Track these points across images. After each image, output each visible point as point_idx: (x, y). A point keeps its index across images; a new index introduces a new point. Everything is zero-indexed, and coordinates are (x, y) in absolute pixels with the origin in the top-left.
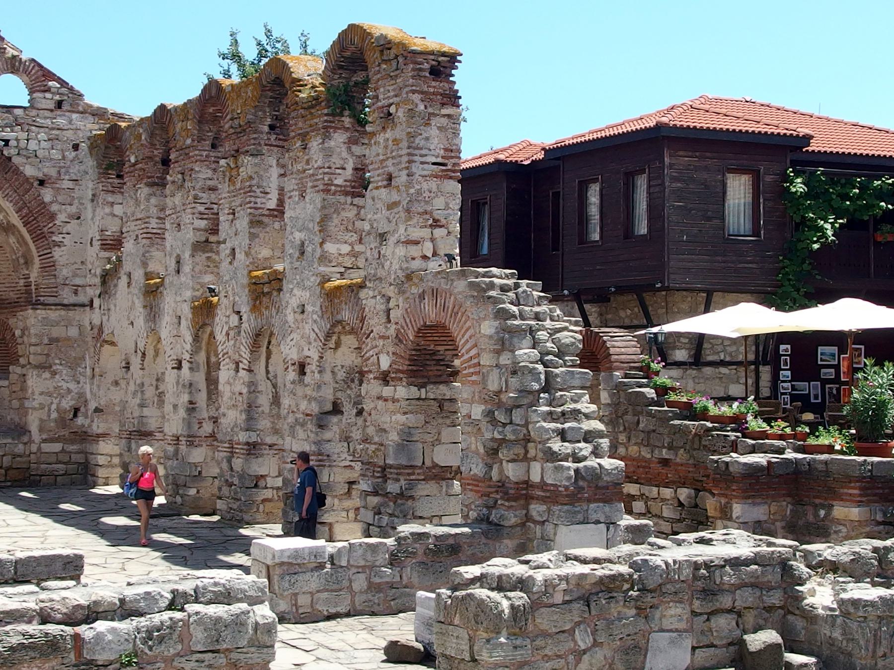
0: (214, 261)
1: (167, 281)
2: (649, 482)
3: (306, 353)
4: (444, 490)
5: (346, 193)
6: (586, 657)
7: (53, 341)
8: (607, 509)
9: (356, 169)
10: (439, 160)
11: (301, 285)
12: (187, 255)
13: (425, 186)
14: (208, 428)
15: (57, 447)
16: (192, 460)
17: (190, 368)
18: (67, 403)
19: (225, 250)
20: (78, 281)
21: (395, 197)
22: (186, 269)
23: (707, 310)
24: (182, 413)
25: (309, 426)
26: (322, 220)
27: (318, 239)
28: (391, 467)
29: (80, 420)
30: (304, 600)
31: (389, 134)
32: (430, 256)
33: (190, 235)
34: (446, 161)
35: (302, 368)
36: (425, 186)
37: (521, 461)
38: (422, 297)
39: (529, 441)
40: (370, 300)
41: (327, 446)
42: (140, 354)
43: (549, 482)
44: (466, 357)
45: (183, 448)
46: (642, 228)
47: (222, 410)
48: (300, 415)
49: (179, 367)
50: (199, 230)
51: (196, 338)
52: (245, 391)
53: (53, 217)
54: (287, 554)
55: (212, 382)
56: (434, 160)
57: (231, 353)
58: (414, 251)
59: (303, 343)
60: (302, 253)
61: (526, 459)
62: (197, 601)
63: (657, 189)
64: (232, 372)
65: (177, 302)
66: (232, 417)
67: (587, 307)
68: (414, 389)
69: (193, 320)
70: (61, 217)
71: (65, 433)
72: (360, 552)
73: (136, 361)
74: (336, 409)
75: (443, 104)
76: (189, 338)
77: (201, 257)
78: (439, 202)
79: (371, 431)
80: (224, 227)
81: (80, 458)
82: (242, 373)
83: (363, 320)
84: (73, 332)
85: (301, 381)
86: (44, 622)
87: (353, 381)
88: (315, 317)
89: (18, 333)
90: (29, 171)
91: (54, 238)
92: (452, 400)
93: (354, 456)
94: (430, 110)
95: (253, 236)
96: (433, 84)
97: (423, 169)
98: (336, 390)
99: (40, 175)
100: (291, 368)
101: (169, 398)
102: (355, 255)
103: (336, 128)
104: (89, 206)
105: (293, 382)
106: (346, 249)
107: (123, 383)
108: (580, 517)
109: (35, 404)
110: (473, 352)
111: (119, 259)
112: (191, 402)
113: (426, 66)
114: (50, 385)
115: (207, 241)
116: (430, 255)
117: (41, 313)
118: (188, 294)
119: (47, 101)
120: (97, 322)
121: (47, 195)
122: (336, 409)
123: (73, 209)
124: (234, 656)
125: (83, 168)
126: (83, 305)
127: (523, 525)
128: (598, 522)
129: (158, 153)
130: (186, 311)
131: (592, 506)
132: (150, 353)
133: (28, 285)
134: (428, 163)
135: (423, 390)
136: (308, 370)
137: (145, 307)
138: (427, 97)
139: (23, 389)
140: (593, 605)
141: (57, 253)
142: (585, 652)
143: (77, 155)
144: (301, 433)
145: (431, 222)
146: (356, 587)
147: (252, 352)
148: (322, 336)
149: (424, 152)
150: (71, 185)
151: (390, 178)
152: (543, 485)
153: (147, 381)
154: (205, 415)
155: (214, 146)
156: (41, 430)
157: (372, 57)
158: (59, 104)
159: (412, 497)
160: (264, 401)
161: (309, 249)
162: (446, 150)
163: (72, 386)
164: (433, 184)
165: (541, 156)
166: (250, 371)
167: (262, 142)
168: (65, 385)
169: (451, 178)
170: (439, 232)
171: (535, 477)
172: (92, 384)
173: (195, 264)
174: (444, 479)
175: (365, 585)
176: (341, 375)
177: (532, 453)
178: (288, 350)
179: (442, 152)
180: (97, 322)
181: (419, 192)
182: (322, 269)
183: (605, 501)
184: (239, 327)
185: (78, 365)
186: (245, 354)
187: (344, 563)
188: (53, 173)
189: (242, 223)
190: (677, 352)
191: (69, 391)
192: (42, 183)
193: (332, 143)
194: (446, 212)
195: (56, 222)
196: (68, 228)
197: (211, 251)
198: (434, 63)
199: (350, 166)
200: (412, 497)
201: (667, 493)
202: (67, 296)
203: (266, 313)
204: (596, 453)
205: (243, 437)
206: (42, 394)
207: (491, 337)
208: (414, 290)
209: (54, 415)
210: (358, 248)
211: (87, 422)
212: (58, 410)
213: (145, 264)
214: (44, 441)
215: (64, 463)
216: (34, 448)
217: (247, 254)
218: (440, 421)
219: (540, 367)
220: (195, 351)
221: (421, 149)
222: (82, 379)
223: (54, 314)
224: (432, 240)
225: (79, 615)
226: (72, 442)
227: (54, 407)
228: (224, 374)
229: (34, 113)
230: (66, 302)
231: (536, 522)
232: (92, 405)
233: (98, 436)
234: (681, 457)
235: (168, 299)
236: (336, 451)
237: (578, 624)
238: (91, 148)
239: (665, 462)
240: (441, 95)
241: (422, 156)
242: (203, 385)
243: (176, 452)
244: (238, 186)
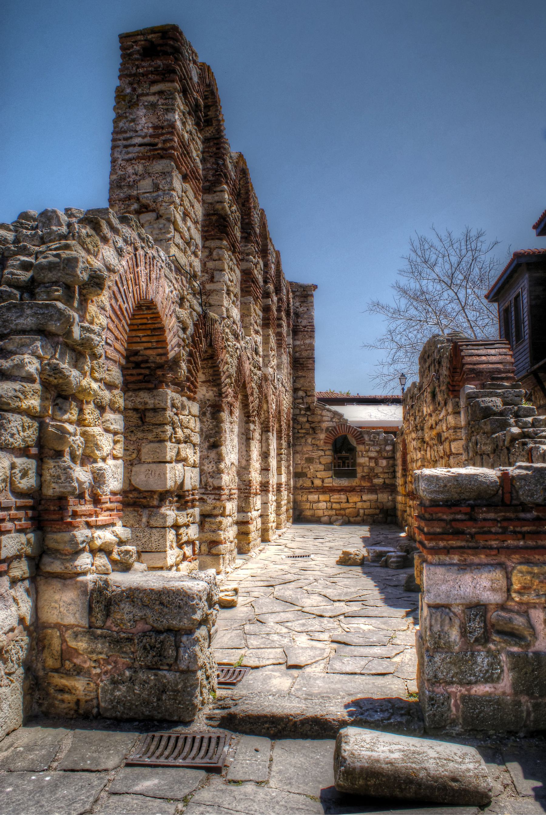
4: (144, 520)
34: (156, 140)
36: (130, 170)
75: (153, 83)
92: (155, 410)
93: (206, 489)
94: (140, 91)
96: (144, 64)
97: (128, 153)
134: (134, 145)
145: (135, 206)
149: (128, 135)
162: (155, 128)
174: (145, 507)
179: (151, 131)
194: (155, 194)
198: (143, 43)
218: (140, 435)
221: (125, 132)
240: (152, 73)
241: (126, 139)
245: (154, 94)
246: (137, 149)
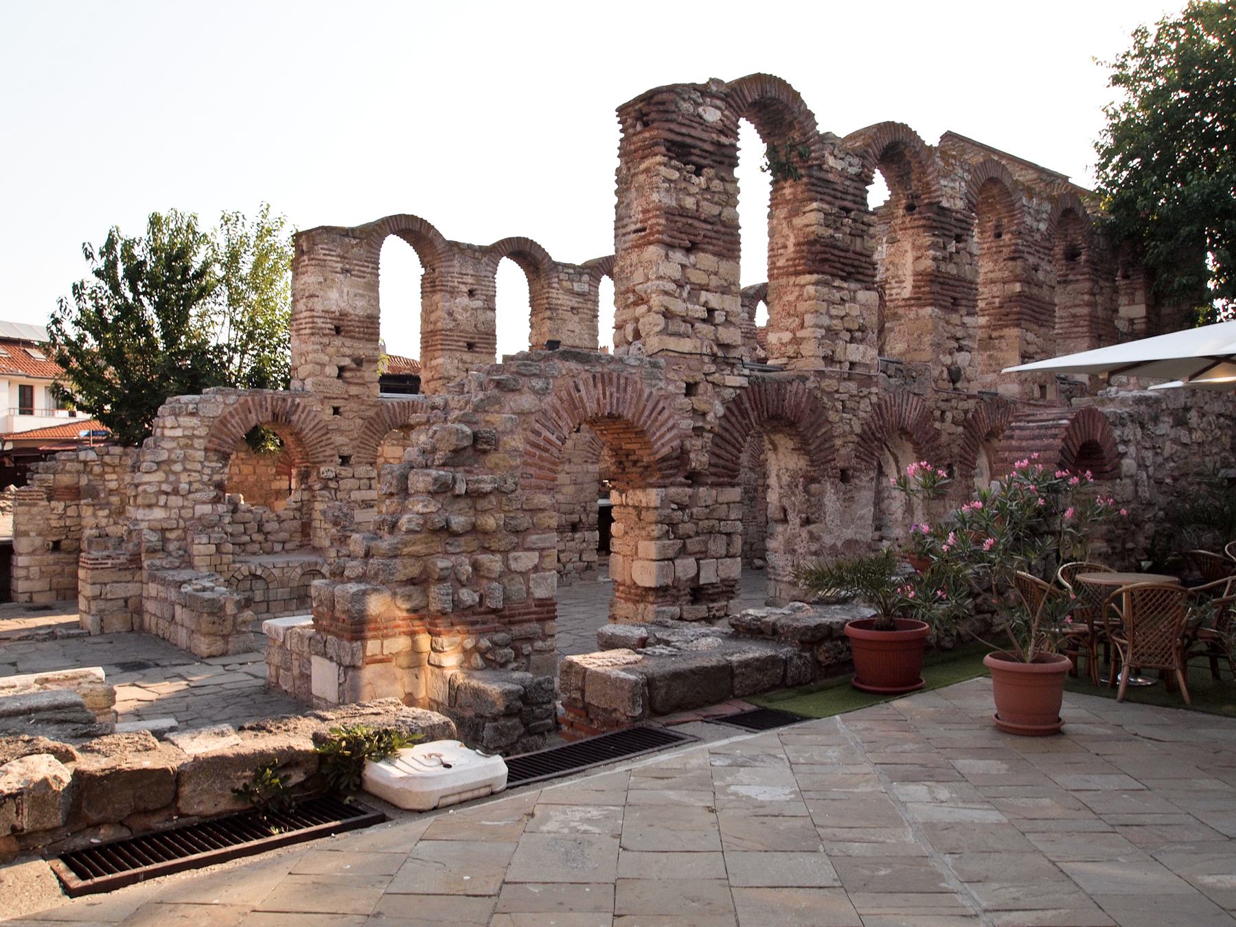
0: (996, 359)
5: (788, 274)
10: (639, 226)
32: (630, 339)
56: (633, 227)
75: (643, 158)
87: (796, 486)
102: (796, 341)
106: (787, 336)
128: (331, 659)
145: (632, 299)
167: (897, 228)
169: (650, 243)
176: (786, 479)
179: (641, 216)
197: (994, 348)
199: (791, 242)
210: (799, 334)
218: (637, 532)
236: (781, 564)
245: (643, 172)
246: (633, 236)
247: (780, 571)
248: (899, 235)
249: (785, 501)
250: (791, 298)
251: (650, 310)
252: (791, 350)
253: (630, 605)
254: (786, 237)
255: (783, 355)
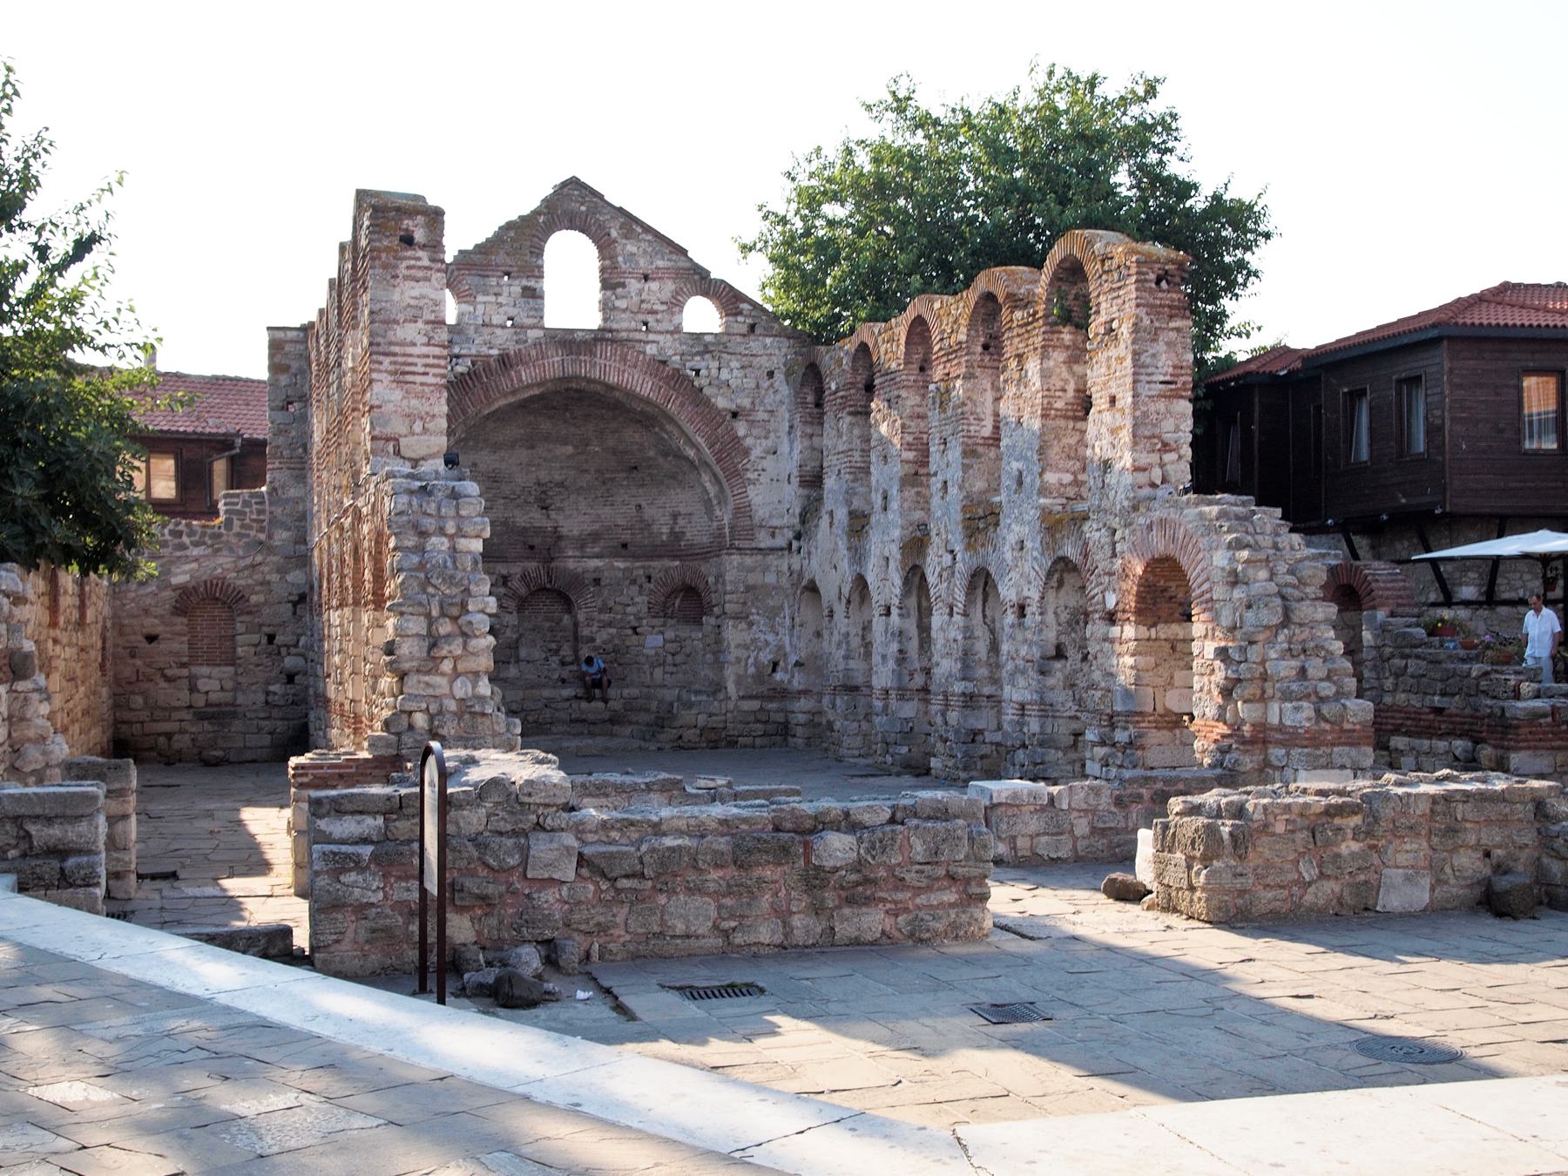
1: (873, 519)
2: (1419, 735)
3: (1026, 593)
5: (1066, 417)
6: (1311, 890)
7: (749, 589)
8: (1354, 752)
9: (1077, 391)
10: (1168, 378)
11: (1019, 520)
12: (894, 491)
13: (1152, 408)
14: (919, 680)
15: (755, 705)
16: (902, 715)
17: (901, 615)
18: (766, 657)
19: (936, 484)
20: (775, 522)
21: (1119, 421)
22: (894, 505)
23: (1500, 536)
24: (891, 664)
25: (1031, 673)
26: (1041, 447)
27: (1037, 469)
28: (1119, 714)
29: (778, 676)
30: (1022, 843)
31: (1113, 352)
32: (1158, 482)
33: (897, 469)
35: (1021, 610)
36: (1152, 408)
37: (1258, 701)
38: (1150, 527)
39: (1265, 680)
40: (1094, 533)
41: (1051, 695)
42: (844, 601)
43: (1288, 723)
44: (1198, 592)
45: (893, 703)
46: (1420, 445)
47: (935, 659)
48: (1020, 662)
49: (888, 613)
50: (907, 462)
51: (906, 581)
52: (960, 637)
53: (746, 452)
54: (1004, 795)
55: (924, 629)
56: (1162, 378)
57: (944, 595)
58: (1142, 478)
59: (1022, 582)
60: (1020, 483)
61: (1263, 699)
62: (915, 815)
63: (1436, 398)
64: (946, 617)
65: (885, 541)
66: (946, 666)
67: (1356, 539)
68: (1143, 629)
69: (902, 561)
70: (756, 453)
71: (763, 689)
72: (1082, 795)
73: (839, 609)
74: (1060, 654)
75: (1171, 317)
76: (898, 582)
77: (910, 493)
78: (1168, 424)
79: (1097, 675)
80: (935, 457)
81: (780, 717)
82: (957, 618)
83: (1086, 556)
84: (770, 578)
85: (1021, 625)
86: (777, 829)
87: (1077, 623)
88: (1035, 554)
89: (711, 580)
90: (721, 402)
91: (749, 475)
94: (1157, 324)
95: (966, 468)
98: (1059, 634)
99: (733, 407)
100: (1009, 611)
101: (877, 649)
103: (1055, 347)
104: (786, 440)
105: (1012, 626)
107: (826, 634)
108: (1323, 761)
109: (731, 658)
110: (1206, 586)
111: (820, 499)
112: (901, 651)
113: (1152, 276)
114: (746, 637)
115: (916, 474)
116: (1158, 482)
117: (736, 559)
118: (896, 533)
119: (742, 323)
120: (796, 567)
121: (741, 428)
122: (1060, 654)
123: (769, 443)
124: (952, 869)
125: (778, 397)
126: (782, 549)
127: (1261, 770)
128: (1343, 767)
129: (861, 379)
130: (894, 551)
131: (1336, 749)
132: (856, 598)
133: (721, 528)
135: (1153, 630)
136: (1028, 610)
137: (849, 549)
138: (1153, 310)
139: (719, 641)
140: (1318, 836)
141: (752, 492)
142: (1310, 884)
143: (772, 385)
144: (1022, 682)
146: (1078, 832)
147: (967, 595)
148: (1043, 574)
149: (1150, 370)
150: (765, 416)
151: (1113, 400)
152: (1281, 728)
153: (853, 632)
154: (917, 665)
155: (922, 369)
156: (738, 683)
157: (1092, 269)
158: (752, 328)
159: (1142, 747)
160: (981, 648)
161: (1028, 480)
162: (1175, 367)
163: (770, 638)
164: (1161, 405)
165: (1298, 365)
166: (965, 614)
168: (762, 637)
170: (1168, 457)
171: (1274, 719)
172: (791, 636)
173: (904, 500)
175: (1087, 830)
176: (1064, 617)
177: (1269, 692)
178: (1008, 592)
180: (796, 567)
181: (1145, 414)
182: (1042, 501)
183: (1351, 745)
184: (952, 567)
185: (777, 615)
186: (960, 596)
187: (1065, 807)
188: (746, 403)
189: (955, 454)
190: (1464, 589)
191: (767, 643)
192: (735, 415)
193: (1051, 363)
195: (752, 458)
196: (765, 464)
197: (921, 484)
199: (1071, 387)
200: (1142, 747)
201: (1441, 745)
202: (764, 541)
203: (981, 551)
204: (1340, 694)
205: (958, 687)
206: (738, 646)
207: (1223, 569)
208: (1141, 520)
209: (751, 670)
210: (1081, 477)
211: (786, 678)
212: (756, 663)
213: (849, 503)
214: (743, 698)
215: (766, 722)
216: (731, 706)
217: (960, 488)
219: (1278, 601)
220: (906, 593)
222: (781, 631)
223: (749, 561)
224: (1162, 465)
225: (808, 824)
226: (771, 699)
227: (751, 661)
228: (937, 620)
229: (725, 338)
230: (762, 545)
231: (1276, 768)
232: (793, 659)
233: (800, 692)
234: (1454, 704)
235: (874, 540)
237: (1302, 854)
238: (788, 374)
239: (1439, 711)
242: (913, 631)
243: (886, 707)
244: (949, 413)
247: (1059, 707)
248: (978, 372)
249: (1063, 638)
250: (1073, 441)
251: (1180, 457)
252: (1071, 492)
253: (1165, 732)
254: (1066, 381)
255: (1061, 496)
